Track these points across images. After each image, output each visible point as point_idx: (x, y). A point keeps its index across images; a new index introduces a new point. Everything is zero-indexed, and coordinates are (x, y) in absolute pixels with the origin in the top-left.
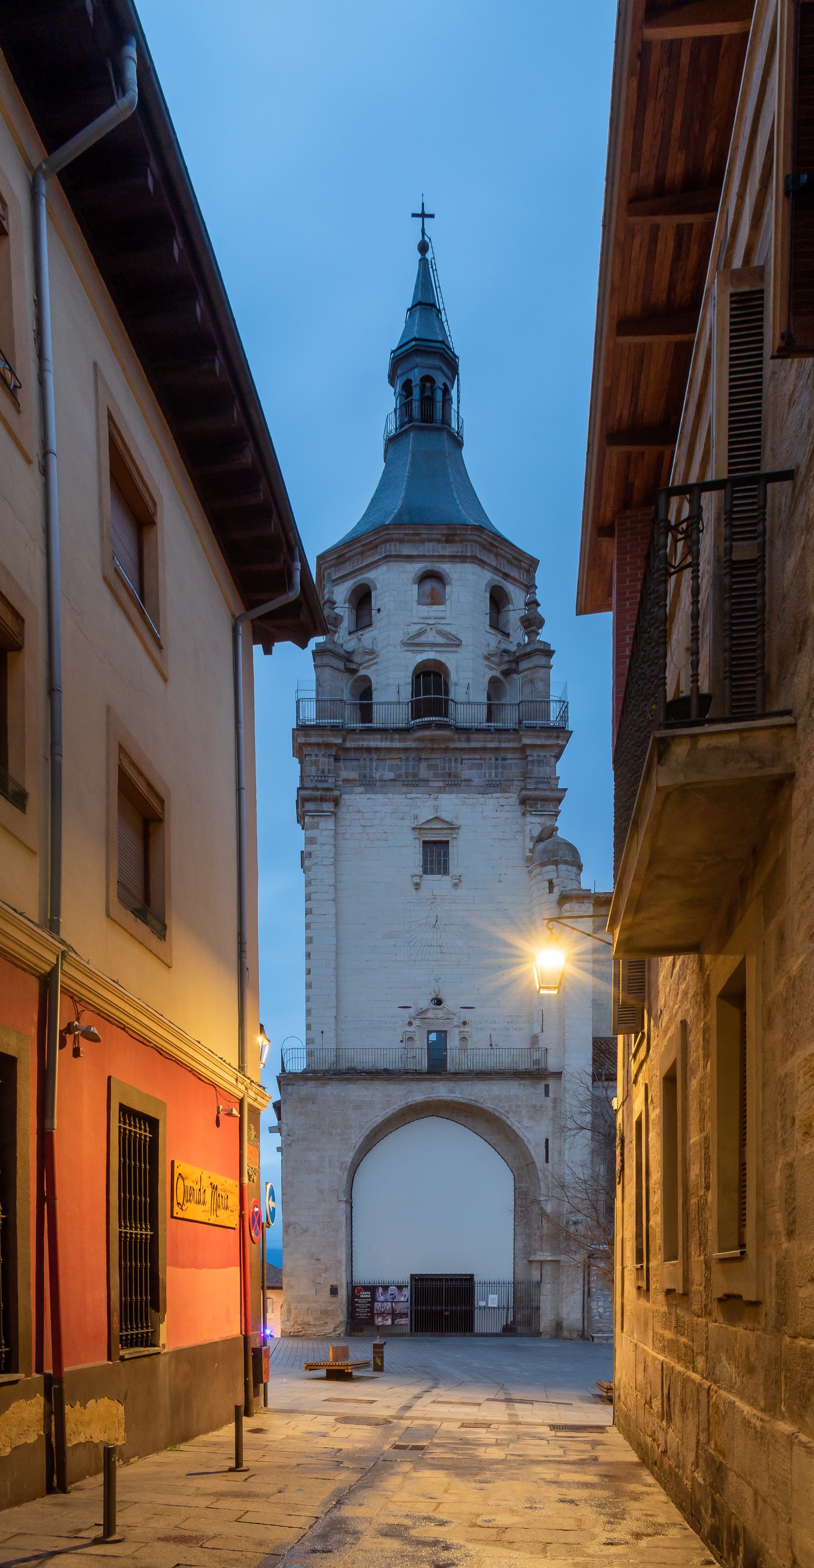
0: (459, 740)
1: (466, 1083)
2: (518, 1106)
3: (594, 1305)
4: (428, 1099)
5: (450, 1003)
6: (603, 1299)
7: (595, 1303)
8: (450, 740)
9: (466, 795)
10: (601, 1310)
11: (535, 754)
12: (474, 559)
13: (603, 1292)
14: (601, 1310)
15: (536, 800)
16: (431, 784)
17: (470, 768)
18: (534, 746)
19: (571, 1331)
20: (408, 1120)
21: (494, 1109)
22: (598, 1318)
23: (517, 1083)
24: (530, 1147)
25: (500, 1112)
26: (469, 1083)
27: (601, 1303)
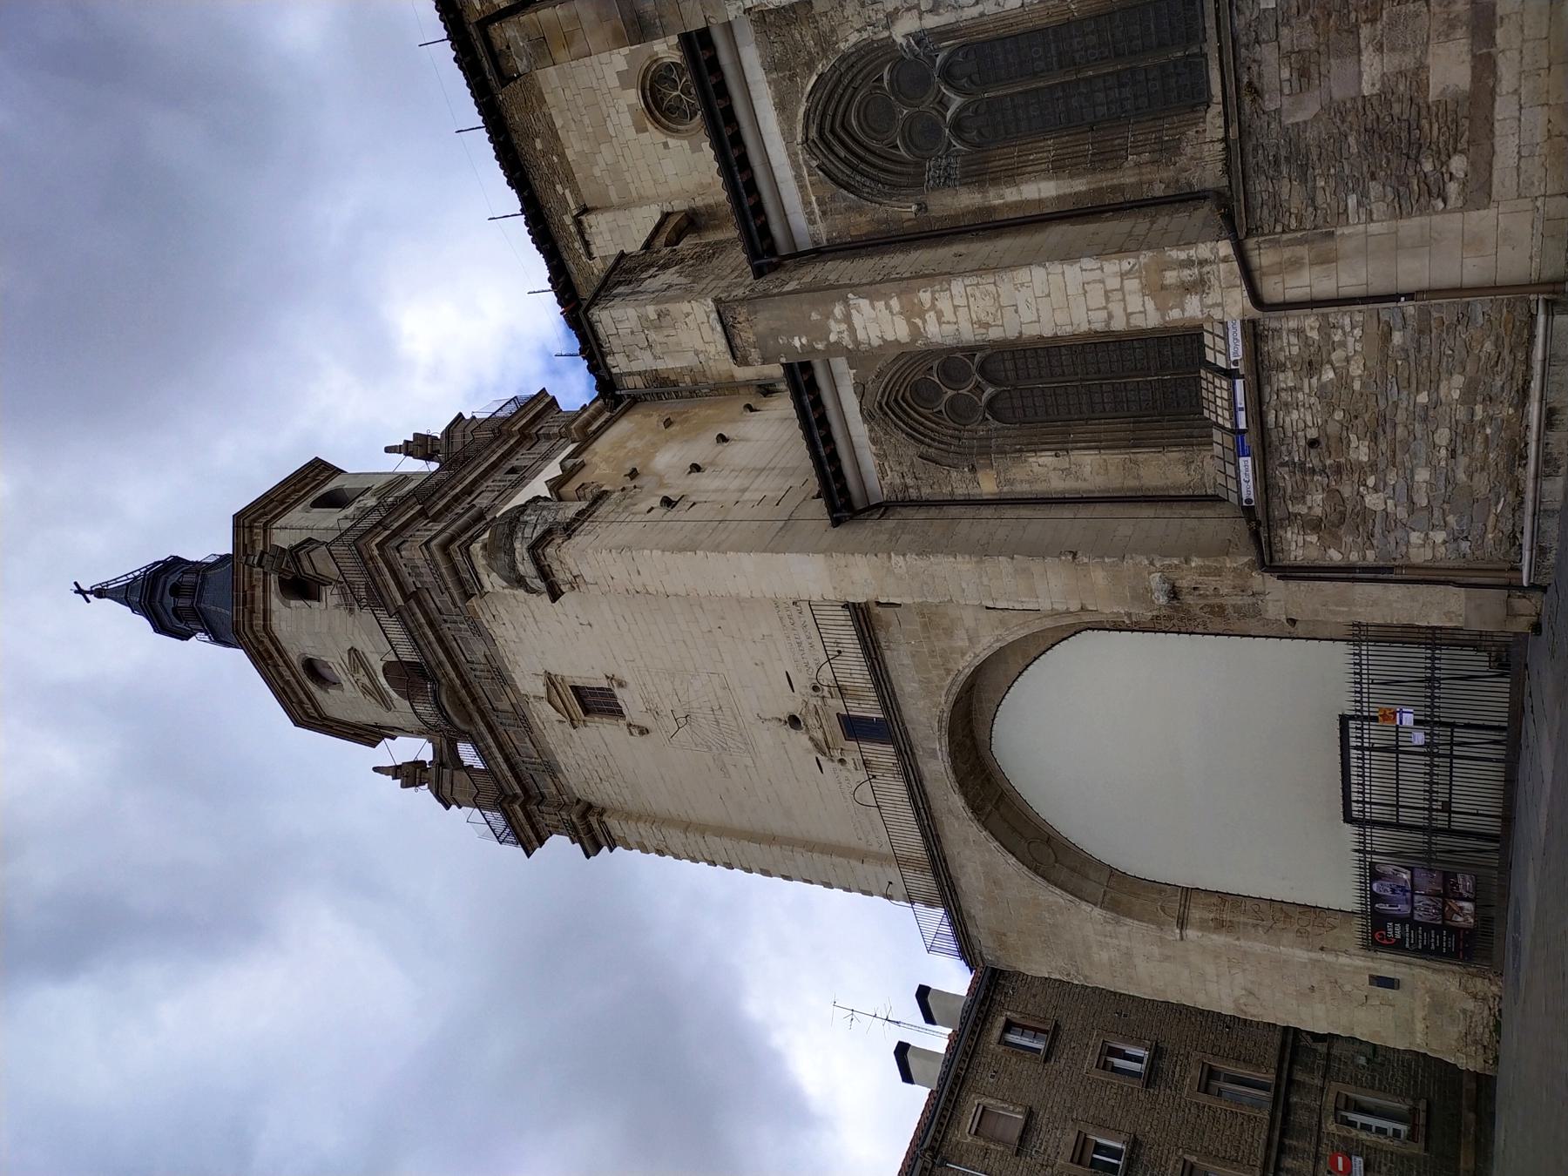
0: (446, 675)
1: (911, 732)
2: (932, 653)
3: (1420, 556)
4: (956, 789)
5: (795, 707)
6: (1399, 533)
7: (1413, 551)
8: (452, 687)
9: (506, 660)
10: (1439, 536)
11: (411, 580)
12: (267, 627)
13: (1377, 530)
14: (1439, 536)
15: (460, 582)
16: (514, 701)
17: (473, 652)
18: (401, 586)
19: (1511, 614)
20: (1008, 786)
21: (947, 695)
22: (1465, 545)
23: (887, 654)
24: (1010, 639)
25: (952, 684)
26: (909, 727)
27: (1416, 538)
